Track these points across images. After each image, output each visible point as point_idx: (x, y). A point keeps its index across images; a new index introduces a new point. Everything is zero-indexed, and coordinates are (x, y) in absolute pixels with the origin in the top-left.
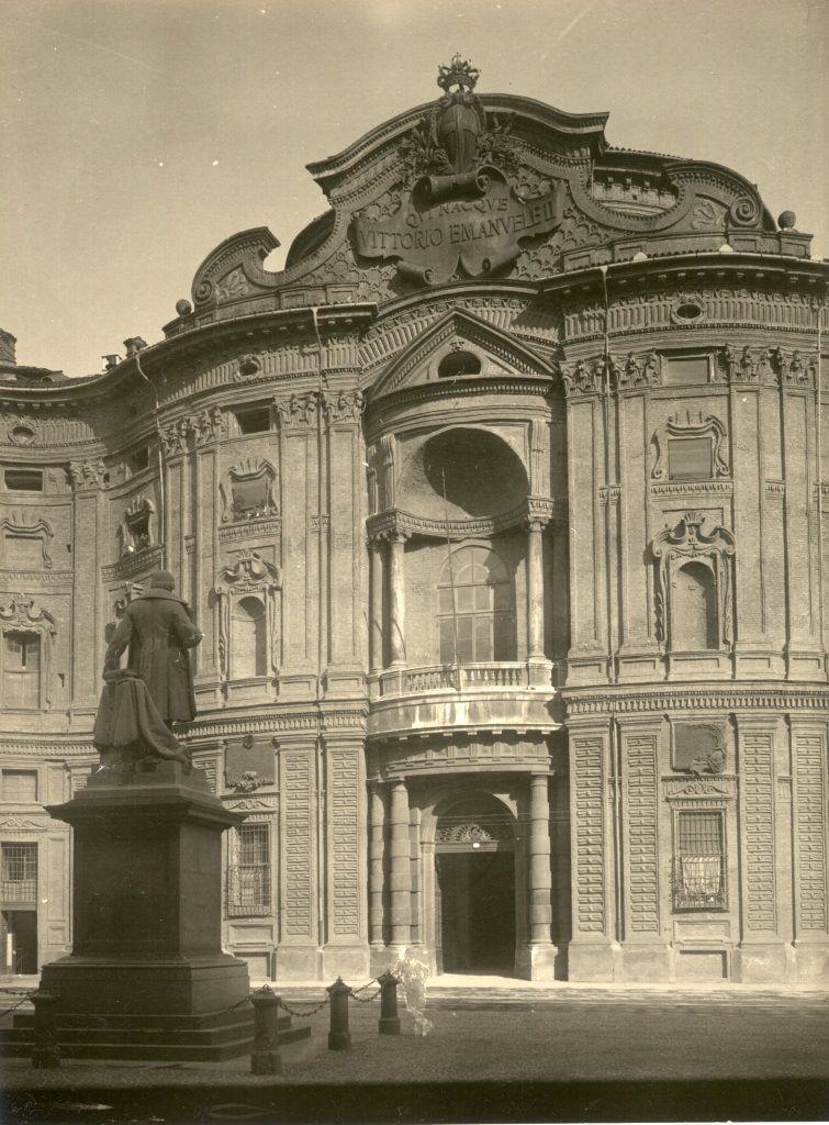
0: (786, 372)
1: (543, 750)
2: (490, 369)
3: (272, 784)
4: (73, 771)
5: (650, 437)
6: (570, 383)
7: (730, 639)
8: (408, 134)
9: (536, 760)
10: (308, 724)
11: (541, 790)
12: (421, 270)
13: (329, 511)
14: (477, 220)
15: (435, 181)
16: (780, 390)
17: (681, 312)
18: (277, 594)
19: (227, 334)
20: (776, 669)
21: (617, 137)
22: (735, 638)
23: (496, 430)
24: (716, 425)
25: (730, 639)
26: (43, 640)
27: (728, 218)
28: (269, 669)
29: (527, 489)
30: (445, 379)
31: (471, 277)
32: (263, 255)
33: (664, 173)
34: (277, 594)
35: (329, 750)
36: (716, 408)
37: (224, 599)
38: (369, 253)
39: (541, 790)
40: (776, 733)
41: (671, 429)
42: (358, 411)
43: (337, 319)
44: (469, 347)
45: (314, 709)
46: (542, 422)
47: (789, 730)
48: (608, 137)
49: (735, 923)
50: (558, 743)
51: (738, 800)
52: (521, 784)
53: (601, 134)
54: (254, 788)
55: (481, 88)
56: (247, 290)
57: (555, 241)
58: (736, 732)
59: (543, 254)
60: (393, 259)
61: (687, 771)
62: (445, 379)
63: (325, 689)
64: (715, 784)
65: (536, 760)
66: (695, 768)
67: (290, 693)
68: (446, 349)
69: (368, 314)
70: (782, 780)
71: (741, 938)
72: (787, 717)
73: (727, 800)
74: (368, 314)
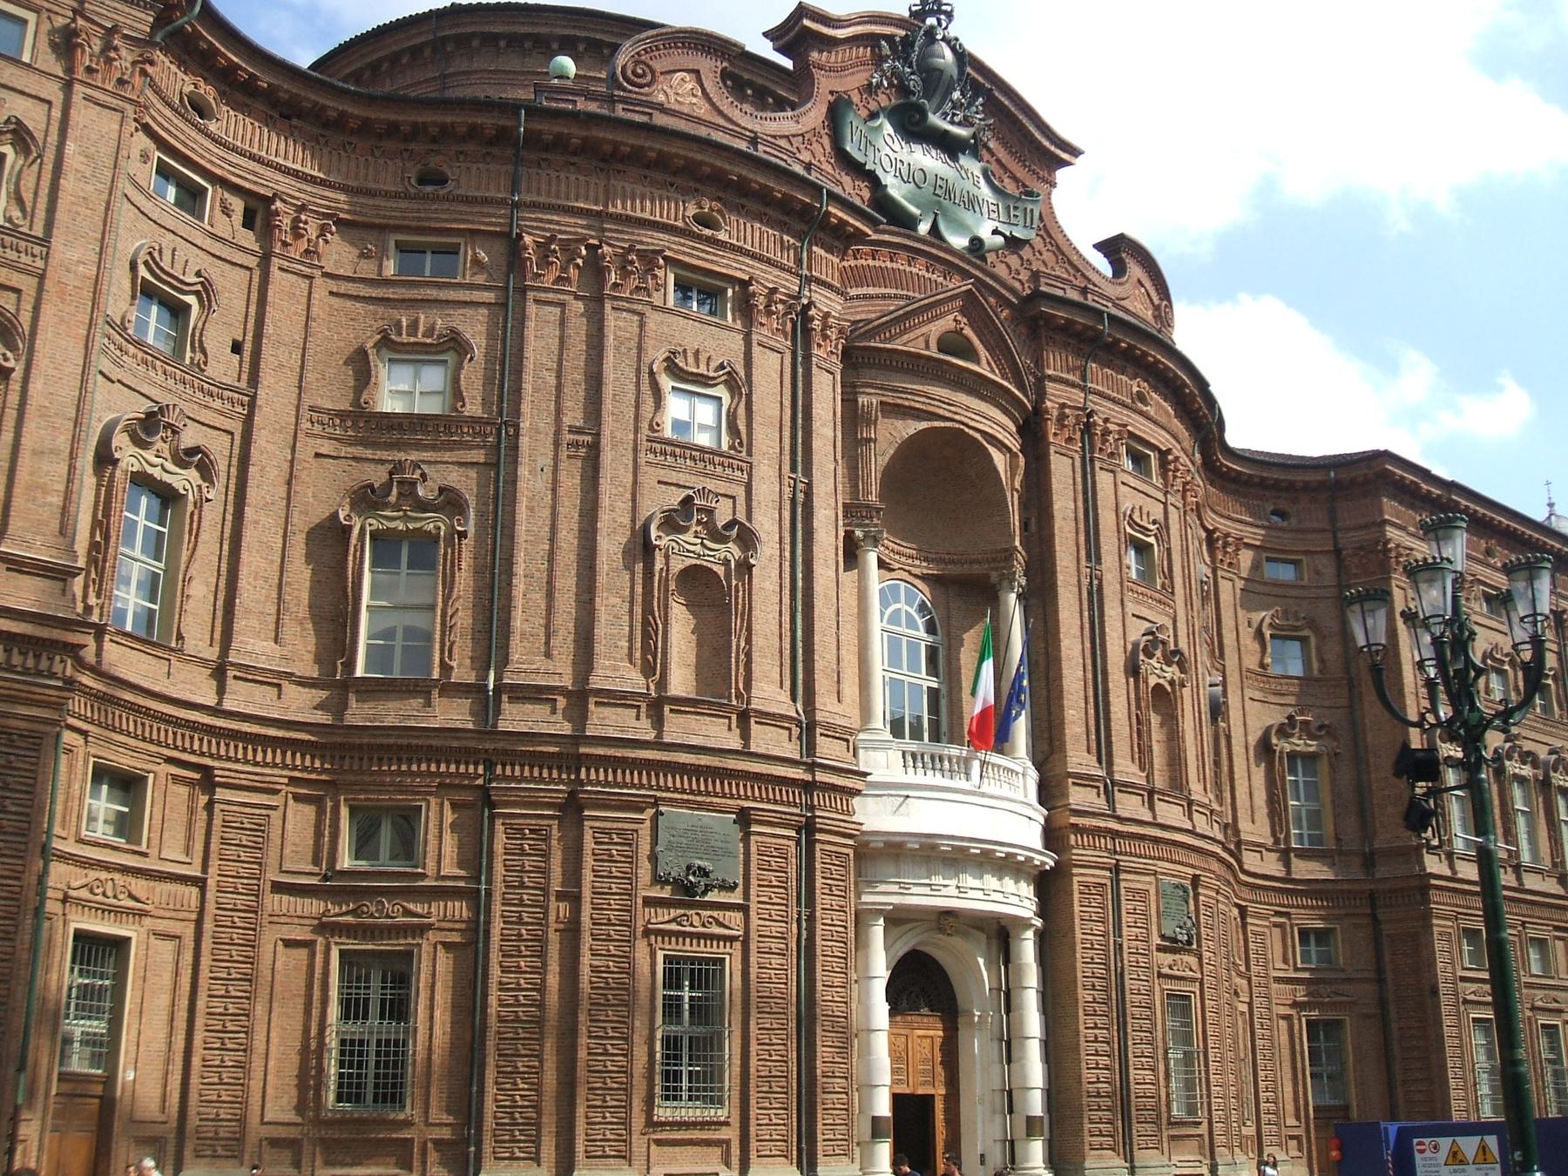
1: (1027, 889)
4: (221, 794)
8: (890, 39)
9: (1016, 899)
10: (508, 772)
11: (1027, 949)
23: (991, 450)
30: (942, 356)
35: (818, 846)
39: (1027, 949)
43: (840, 219)
44: (968, 331)
50: (1049, 886)
52: (1000, 933)
59: (1013, 260)
61: (1175, 940)
62: (942, 356)
65: (1016, 899)
68: (946, 323)
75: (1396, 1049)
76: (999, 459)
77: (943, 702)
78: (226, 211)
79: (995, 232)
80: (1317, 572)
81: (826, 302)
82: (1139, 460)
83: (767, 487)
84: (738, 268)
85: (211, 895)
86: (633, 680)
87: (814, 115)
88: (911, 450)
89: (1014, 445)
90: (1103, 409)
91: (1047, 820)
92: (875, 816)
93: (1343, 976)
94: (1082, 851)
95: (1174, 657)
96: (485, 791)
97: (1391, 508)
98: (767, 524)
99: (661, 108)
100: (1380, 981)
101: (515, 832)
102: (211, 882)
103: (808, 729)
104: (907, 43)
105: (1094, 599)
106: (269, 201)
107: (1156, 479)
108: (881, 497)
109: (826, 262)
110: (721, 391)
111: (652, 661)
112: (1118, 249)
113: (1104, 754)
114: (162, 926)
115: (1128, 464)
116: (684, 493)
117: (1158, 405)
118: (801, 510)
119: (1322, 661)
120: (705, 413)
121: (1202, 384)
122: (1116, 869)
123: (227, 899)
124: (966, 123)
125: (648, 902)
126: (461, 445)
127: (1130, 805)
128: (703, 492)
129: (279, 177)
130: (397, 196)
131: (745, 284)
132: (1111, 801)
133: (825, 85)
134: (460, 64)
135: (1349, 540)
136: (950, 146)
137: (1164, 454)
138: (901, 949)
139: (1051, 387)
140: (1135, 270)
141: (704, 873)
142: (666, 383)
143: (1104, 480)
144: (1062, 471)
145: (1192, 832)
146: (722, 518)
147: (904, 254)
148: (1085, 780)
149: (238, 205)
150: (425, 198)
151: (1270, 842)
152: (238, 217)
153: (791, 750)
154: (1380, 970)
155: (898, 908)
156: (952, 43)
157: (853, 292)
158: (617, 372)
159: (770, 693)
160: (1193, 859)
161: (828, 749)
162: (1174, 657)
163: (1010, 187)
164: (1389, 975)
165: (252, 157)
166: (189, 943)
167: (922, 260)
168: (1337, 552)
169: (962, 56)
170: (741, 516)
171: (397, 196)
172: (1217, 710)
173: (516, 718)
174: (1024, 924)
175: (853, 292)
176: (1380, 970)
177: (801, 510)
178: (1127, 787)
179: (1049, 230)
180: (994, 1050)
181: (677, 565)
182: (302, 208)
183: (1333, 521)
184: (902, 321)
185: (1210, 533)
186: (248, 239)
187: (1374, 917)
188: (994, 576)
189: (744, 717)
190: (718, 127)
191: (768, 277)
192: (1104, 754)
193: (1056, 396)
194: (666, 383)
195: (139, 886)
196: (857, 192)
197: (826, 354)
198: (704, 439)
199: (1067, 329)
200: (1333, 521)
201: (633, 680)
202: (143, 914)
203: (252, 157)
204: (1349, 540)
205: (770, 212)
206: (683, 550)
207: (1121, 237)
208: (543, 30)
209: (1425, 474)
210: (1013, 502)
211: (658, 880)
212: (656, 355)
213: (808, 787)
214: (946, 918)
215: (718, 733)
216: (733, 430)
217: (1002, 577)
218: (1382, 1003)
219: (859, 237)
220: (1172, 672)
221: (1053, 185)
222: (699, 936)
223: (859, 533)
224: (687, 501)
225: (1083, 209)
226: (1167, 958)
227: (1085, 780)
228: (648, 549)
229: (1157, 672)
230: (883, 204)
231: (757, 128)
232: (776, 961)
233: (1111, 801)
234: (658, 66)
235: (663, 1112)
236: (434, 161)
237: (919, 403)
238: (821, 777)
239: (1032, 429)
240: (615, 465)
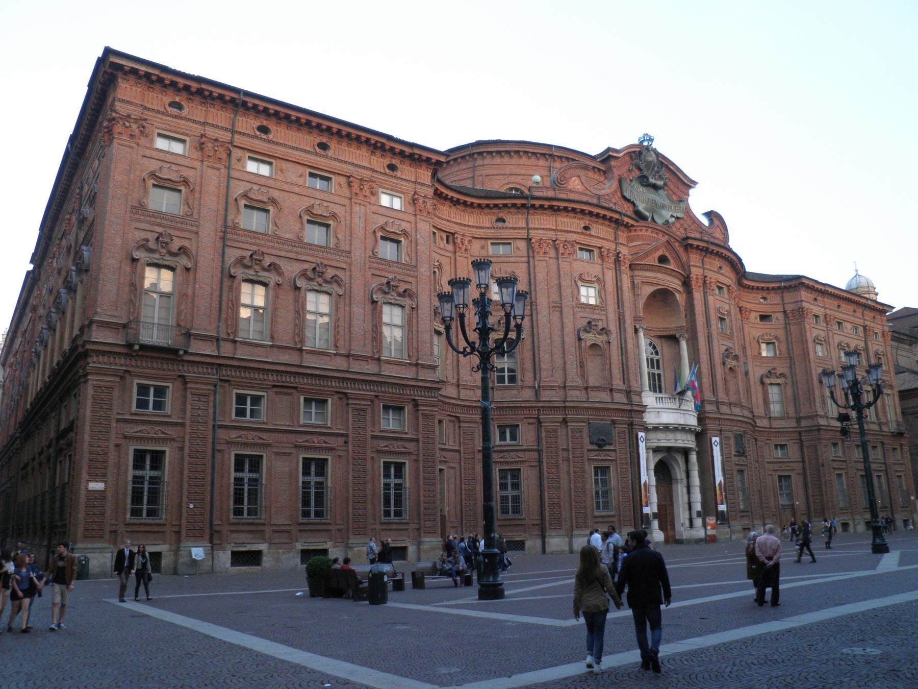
1: (693, 438)
3: (611, 444)
6: (693, 283)
8: (635, 152)
9: (689, 442)
11: (693, 457)
14: (657, 198)
38: (627, 195)
39: (693, 457)
44: (667, 254)
45: (629, 408)
50: (700, 436)
52: (685, 452)
54: (605, 445)
57: (682, 221)
59: (678, 225)
65: (689, 442)
68: (660, 253)
75: (809, 485)
76: (677, 295)
77: (662, 378)
78: (442, 239)
79: (672, 216)
81: (624, 251)
82: (720, 288)
83: (612, 316)
84: (597, 243)
85: (462, 454)
86: (579, 382)
87: (614, 184)
88: (654, 295)
89: (681, 289)
90: (709, 274)
91: (698, 415)
92: (650, 418)
94: (711, 426)
95: (736, 358)
96: (538, 419)
97: (804, 294)
98: (613, 327)
99: (570, 191)
100: (803, 462)
101: (547, 431)
103: (628, 393)
104: (640, 153)
105: (709, 337)
106: (453, 234)
107: (726, 296)
108: (644, 313)
109: (623, 236)
110: (596, 285)
111: (583, 375)
112: (710, 215)
113: (714, 391)
115: (717, 291)
116: (587, 320)
117: (727, 270)
118: (621, 320)
120: (592, 292)
121: (740, 260)
122: (721, 431)
123: (467, 456)
124: (661, 178)
125: (588, 450)
127: (724, 409)
128: (594, 320)
129: (455, 226)
130: (490, 228)
131: (600, 248)
132: (718, 408)
133: (616, 172)
134: (479, 162)
135: (789, 308)
136: (655, 187)
137: (728, 286)
138: (657, 460)
139: (693, 269)
140: (716, 222)
141: (603, 440)
142: (580, 283)
143: (711, 299)
144: (698, 296)
145: (743, 416)
146: (600, 327)
147: (644, 229)
148: (710, 402)
149: (444, 235)
150: (498, 228)
151: (764, 415)
152: (445, 241)
153: (625, 400)
154: (803, 457)
155: (657, 447)
156: (655, 151)
157: (631, 245)
158: (565, 281)
159: (617, 383)
160: (744, 425)
161: (635, 398)
162: (736, 358)
163: (675, 198)
164: (806, 459)
165: (448, 221)
166: (458, 469)
167: (650, 230)
168: (785, 312)
169: (658, 155)
170: (605, 326)
171: (490, 228)
172: (747, 374)
173: (545, 396)
174: (690, 449)
175: (631, 245)
176: (803, 457)
177: (621, 320)
178: (723, 403)
179: (688, 212)
180: (685, 490)
181: (588, 344)
182: (463, 235)
183: (783, 300)
184: (648, 254)
185: (740, 308)
186: (450, 247)
187: (800, 439)
188: (678, 336)
189: (611, 390)
190: (586, 195)
191: (607, 245)
192: (714, 391)
193: (696, 272)
194: (580, 283)
196: (627, 209)
197: (625, 268)
198: (592, 301)
200: (783, 300)
201: (579, 382)
202: (446, 462)
203: (448, 221)
204: (789, 308)
206: (590, 338)
207: (712, 212)
208: (508, 149)
209: (817, 282)
210: (682, 309)
211: (592, 443)
212: (576, 275)
213: (630, 411)
214: (669, 449)
215: (604, 396)
216: (600, 297)
217: (680, 336)
218: (804, 469)
219: (632, 226)
220: (734, 363)
221: (688, 195)
222: (603, 460)
223: (637, 326)
224: (589, 323)
225: (699, 203)
226: (737, 459)
227: (710, 402)
228: (580, 339)
229: (731, 363)
230: (640, 216)
231: (599, 193)
232: (625, 466)
233: (718, 408)
234: (567, 176)
235: (597, 513)
236: (500, 215)
237: (654, 281)
238: (634, 408)
239: (687, 283)
240: (567, 312)
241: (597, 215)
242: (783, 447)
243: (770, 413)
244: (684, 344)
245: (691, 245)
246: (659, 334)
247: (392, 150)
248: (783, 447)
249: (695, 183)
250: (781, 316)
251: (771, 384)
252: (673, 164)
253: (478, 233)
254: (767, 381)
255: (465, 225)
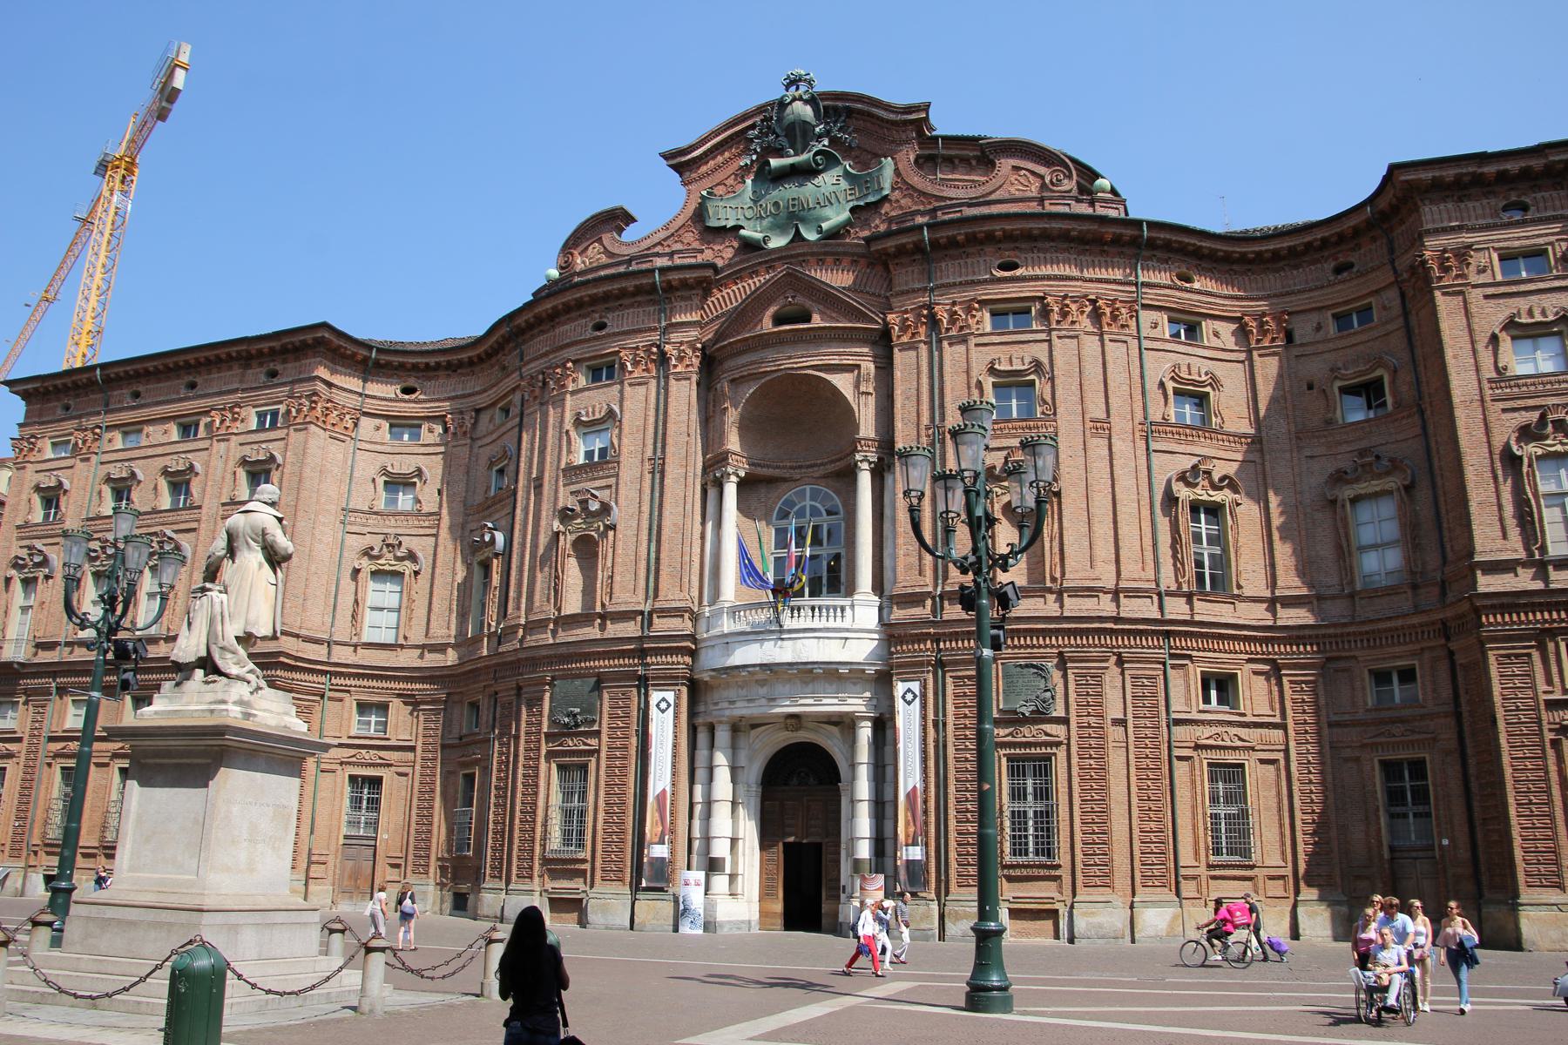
0: (1106, 319)
2: (817, 321)
5: (974, 381)
7: (1058, 575)
8: (753, 127)
12: (759, 236)
13: (663, 451)
15: (774, 162)
16: (1101, 335)
17: (1003, 267)
18: (611, 533)
19: (586, 308)
20: (1106, 606)
21: (944, 123)
22: (1063, 574)
24: (1037, 366)
25: (1058, 575)
26: (407, 578)
27: (1043, 186)
28: (599, 604)
29: (857, 428)
31: (804, 239)
32: (620, 231)
33: (983, 152)
34: (611, 533)
36: (1040, 352)
37: (562, 538)
38: (713, 223)
40: (1107, 678)
41: (992, 371)
42: (696, 362)
44: (800, 299)
46: (869, 367)
47: (1122, 674)
48: (933, 120)
49: (1067, 879)
51: (1068, 745)
52: (846, 724)
53: (926, 119)
54: (577, 725)
55: (820, 87)
56: (604, 259)
57: (886, 208)
58: (1065, 676)
60: (738, 228)
63: (650, 624)
64: (1048, 727)
66: (1023, 710)
67: (614, 630)
69: (709, 273)
70: (1116, 722)
71: (1074, 895)
72: (1120, 662)
73: (1058, 744)
74: (709, 273)
80: (1385, 308)
93: (1422, 711)
97: (1431, 214)
100: (1458, 716)
102: (419, 750)
114: (400, 770)
119: (1394, 395)
126: (504, 507)
147: (762, 269)
164: (1465, 708)
195: (382, 753)
199: (901, 251)
205: (639, 299)
241: (607, 297)
242: (1407, 676)
243: (1352, 582)
244: (865, 480)
245: (885, 252)
246: (831, 468)
247: (260, 353)
248: (1407, 676)
249: (926, 107)
250: (1392, 295)
251: (1355, 501)
252: (860, 98)
253: (482, 400)
254: (1348, 492)
255: (470, 395)
